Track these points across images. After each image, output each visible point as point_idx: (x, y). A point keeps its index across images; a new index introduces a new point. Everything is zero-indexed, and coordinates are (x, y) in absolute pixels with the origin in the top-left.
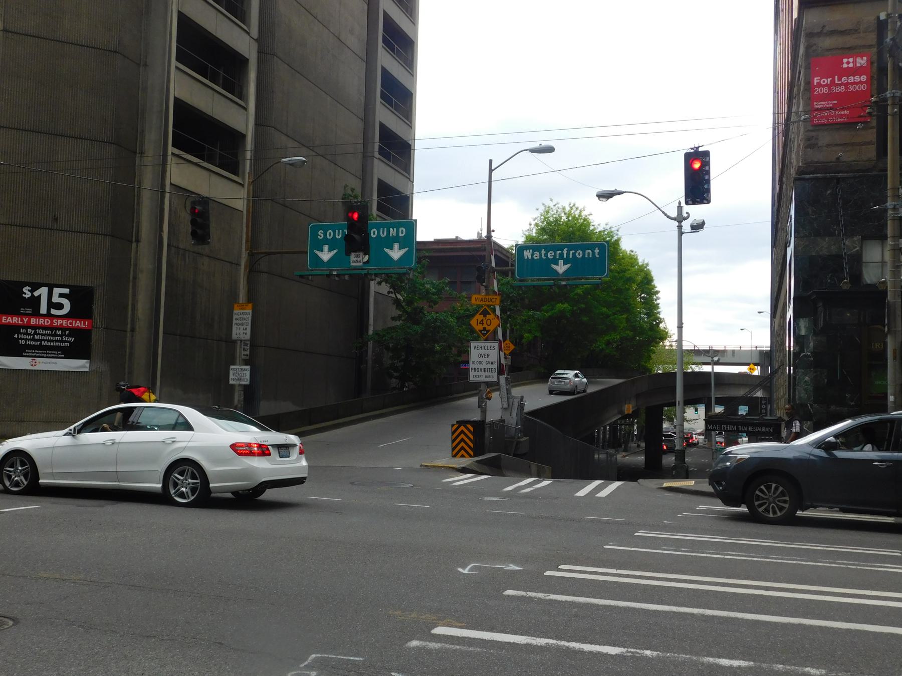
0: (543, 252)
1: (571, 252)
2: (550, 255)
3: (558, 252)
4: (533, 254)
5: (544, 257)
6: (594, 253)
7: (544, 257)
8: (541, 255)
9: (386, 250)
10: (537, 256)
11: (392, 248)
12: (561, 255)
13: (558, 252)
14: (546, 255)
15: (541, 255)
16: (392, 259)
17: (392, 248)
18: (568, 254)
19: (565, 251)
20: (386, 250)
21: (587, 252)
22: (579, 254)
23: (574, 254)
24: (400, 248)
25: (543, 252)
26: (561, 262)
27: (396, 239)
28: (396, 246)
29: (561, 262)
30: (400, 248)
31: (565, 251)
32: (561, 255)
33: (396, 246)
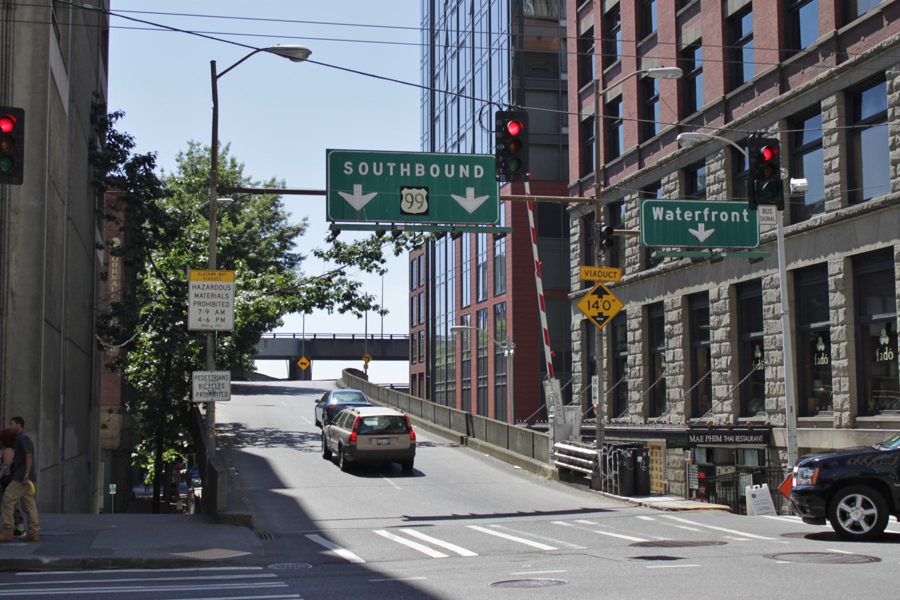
0: (678, 212)
1: (714, 213)
2: (688, 215)
3: (697, 213)
4: (665, 214)
5: (679, 218)
6: (742, 217)
7: (679, 218)
8: (675, 215)
9: (454, 197)
10: (670, 216)
11: (463, 194)
12: (701, 216)
13: (697, 213)
14: (682, 215)
15: (675, 215)
16: (463, 210)
17: (463, 194)
18: (710, 216)
19: (706, 212)
20: (454, 197)
21: (733, 214)
22: (724, 216)
23: (717, 217)
24: (477, 195)
25: (678, 212)
26: (701, 226)
27: (470, 181)
28: (470, 191)
29: (701, 226)
30: (477, 195)
31: (706, 212)
32: (701, 216)
33: (470, 191)
